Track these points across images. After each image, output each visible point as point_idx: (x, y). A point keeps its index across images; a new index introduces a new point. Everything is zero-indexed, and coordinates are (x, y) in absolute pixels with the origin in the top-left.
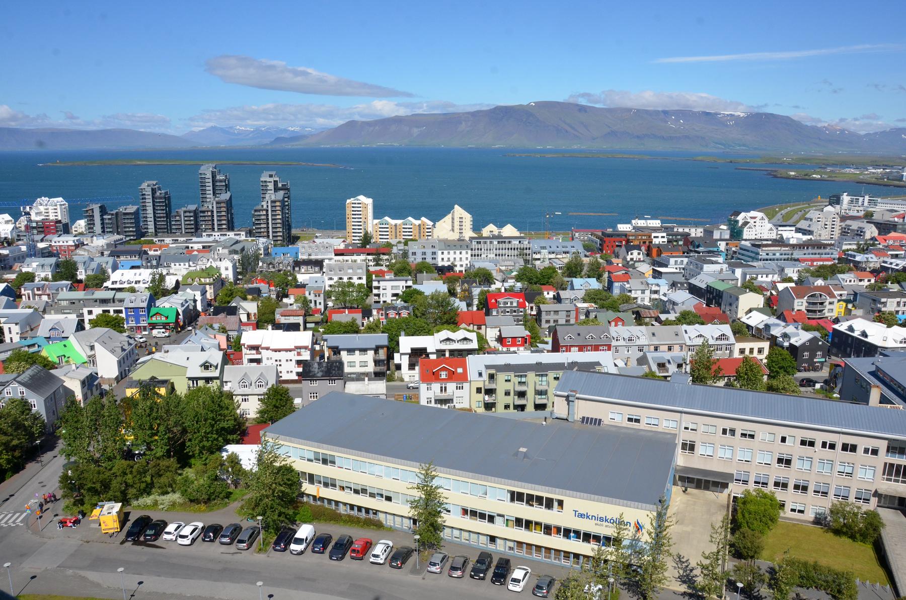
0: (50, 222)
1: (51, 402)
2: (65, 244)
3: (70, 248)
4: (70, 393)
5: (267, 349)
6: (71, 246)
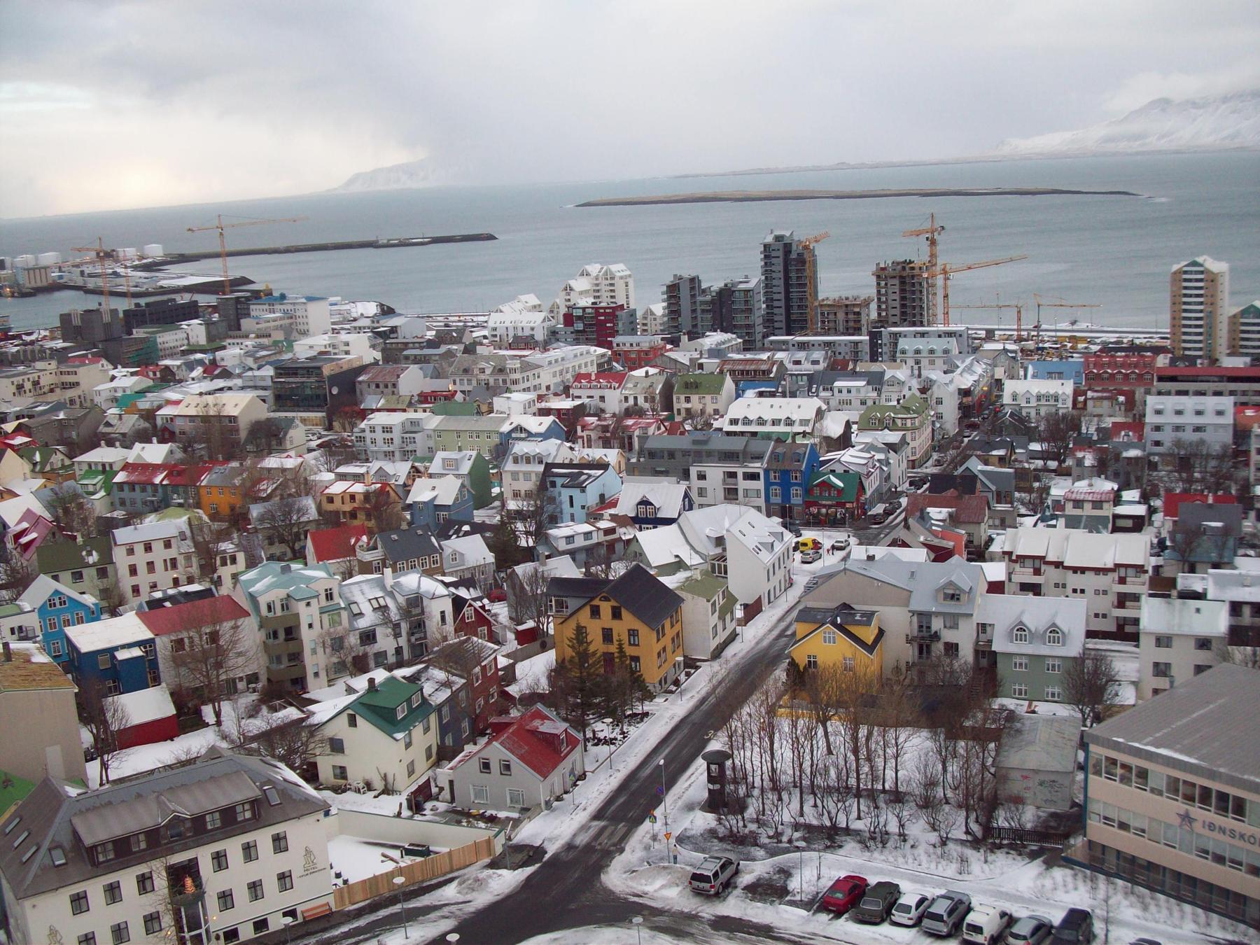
5: (1058, 565)
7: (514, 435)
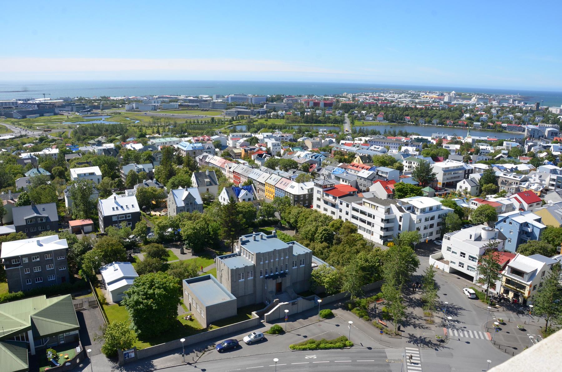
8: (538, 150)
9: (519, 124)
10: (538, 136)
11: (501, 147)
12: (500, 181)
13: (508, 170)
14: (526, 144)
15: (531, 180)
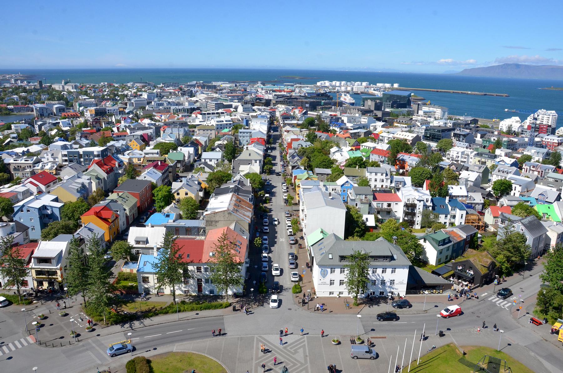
0: (544, 126)
1: (537, 241)
2: (552, 141)
3: (554, 144)
4: (548, 239)
6: (556, 143)
7: (500, 163)
8: (49, 128)
9: (26, 104)
10: (47, 114)
11: (10, 131)
12: (12, 168)
13: (19, 154)
14: (36, 124)
15: (44, 160)
